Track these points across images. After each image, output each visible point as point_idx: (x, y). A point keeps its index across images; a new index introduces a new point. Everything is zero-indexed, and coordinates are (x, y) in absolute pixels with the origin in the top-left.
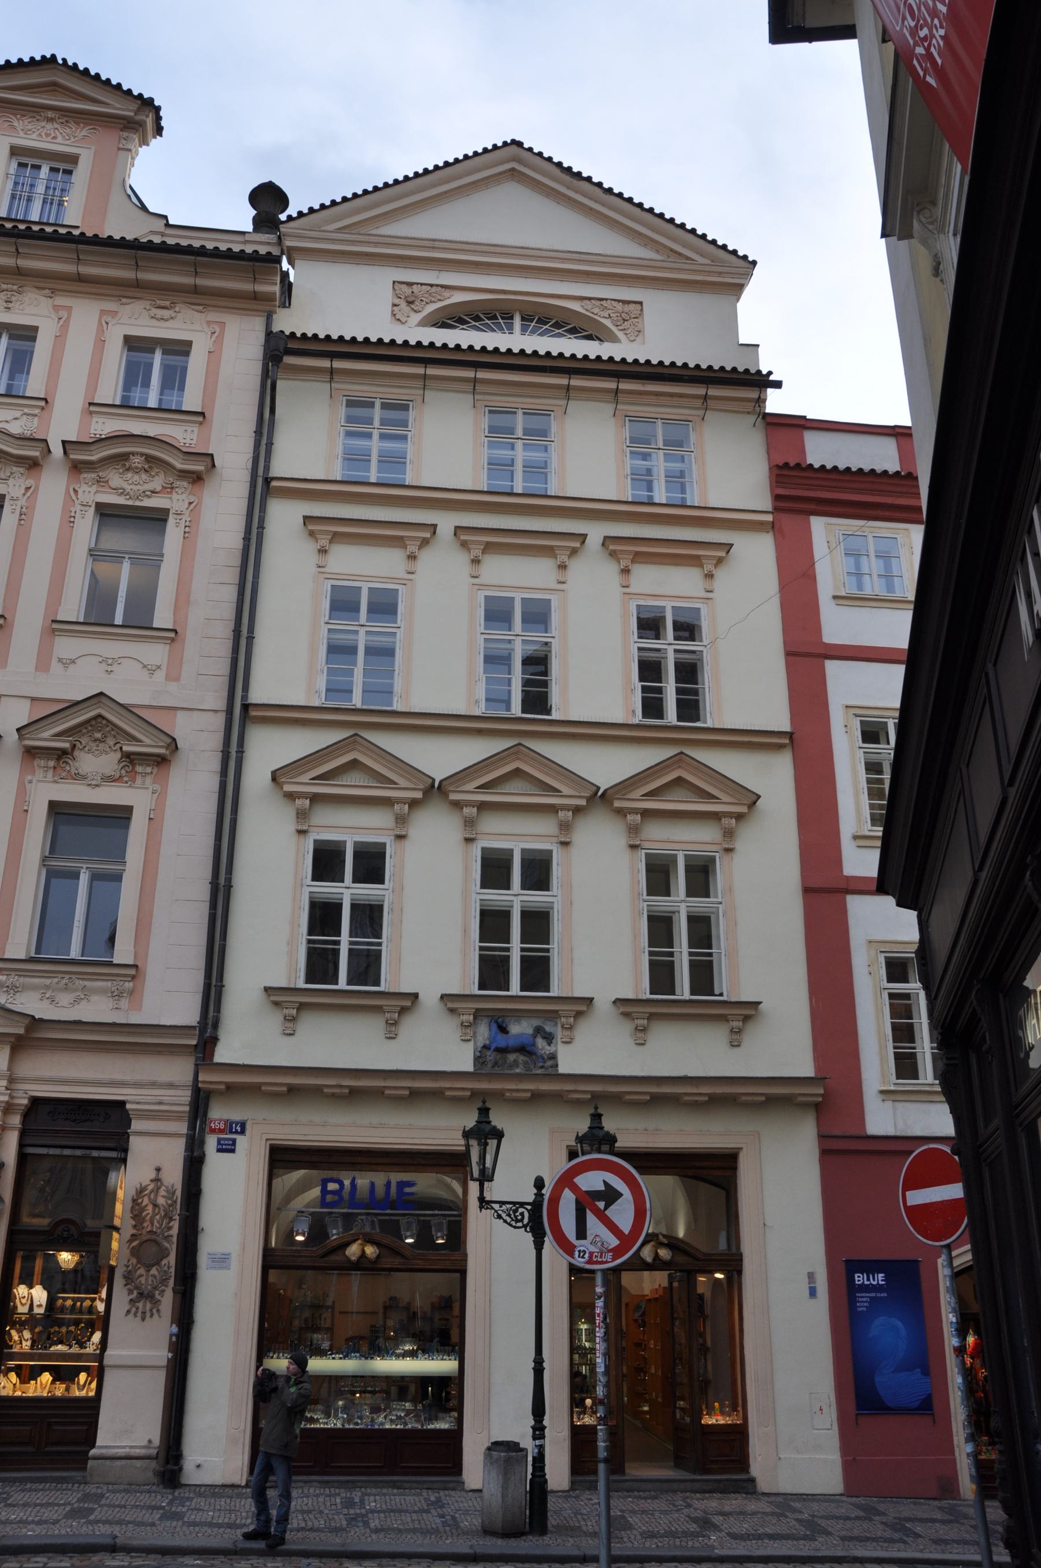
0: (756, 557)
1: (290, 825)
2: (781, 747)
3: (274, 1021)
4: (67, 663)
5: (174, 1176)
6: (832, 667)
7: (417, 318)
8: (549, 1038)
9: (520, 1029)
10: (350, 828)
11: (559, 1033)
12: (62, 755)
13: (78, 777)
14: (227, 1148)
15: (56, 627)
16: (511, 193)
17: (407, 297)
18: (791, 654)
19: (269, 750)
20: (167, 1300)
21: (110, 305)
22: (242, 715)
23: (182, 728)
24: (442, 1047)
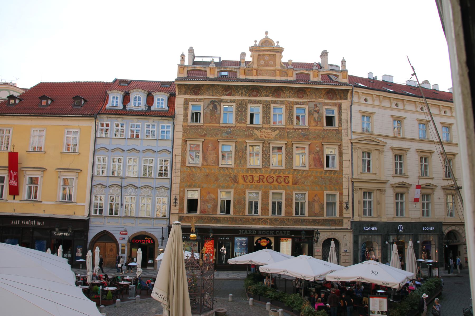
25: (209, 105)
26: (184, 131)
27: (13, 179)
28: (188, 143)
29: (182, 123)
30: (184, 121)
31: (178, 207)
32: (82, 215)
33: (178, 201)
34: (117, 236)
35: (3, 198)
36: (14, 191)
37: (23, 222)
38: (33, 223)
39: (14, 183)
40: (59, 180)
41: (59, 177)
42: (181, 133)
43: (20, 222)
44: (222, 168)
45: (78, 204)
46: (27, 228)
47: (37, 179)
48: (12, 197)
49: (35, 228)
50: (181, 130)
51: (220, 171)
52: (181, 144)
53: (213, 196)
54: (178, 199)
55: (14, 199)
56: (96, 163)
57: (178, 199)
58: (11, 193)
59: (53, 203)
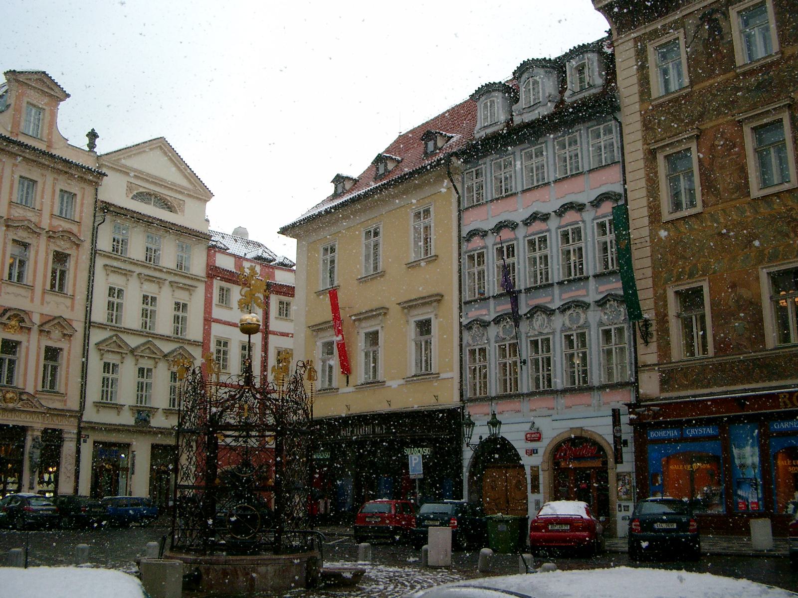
0: (201, 289)
1: (99, 357)
2: (199, 345)
3: (95, 410)
4: (48, 303)
5: (74, 449)
6: (213, 324)
7: (131, 195)
8: (149, 417)
9: (144, 415)
10: (112, 359)
11: (151, 415)
12: (48, 332)
13: (50, 339)
14: (85, 441)
15: (44, 292)
16: (158, 152)
17: (130, 188)
18: (205, 320)
19: (97, 336)
20: (73, 478)
21: (56, 176)
22: (89, 325)
23: (75, 325)
24: (127, 419)
25: (699, 27)
26: (647, 126)
28: (660, 158)
29: (637, 107)
30: (642, 101)
31: (653, 347)
32: (450, 398)
33: (653, 329)
34: (521, 446)
42: (639, 135)
44: (764, 198)
45: (442, 376)
47: (377, 332)
50: (638, 126)
51: (756, 212)
52: (641, 164)
53: (745, 293)
54: (654, 323)
56: (465, 271)
57: (654, 323)
59: (402, 382)
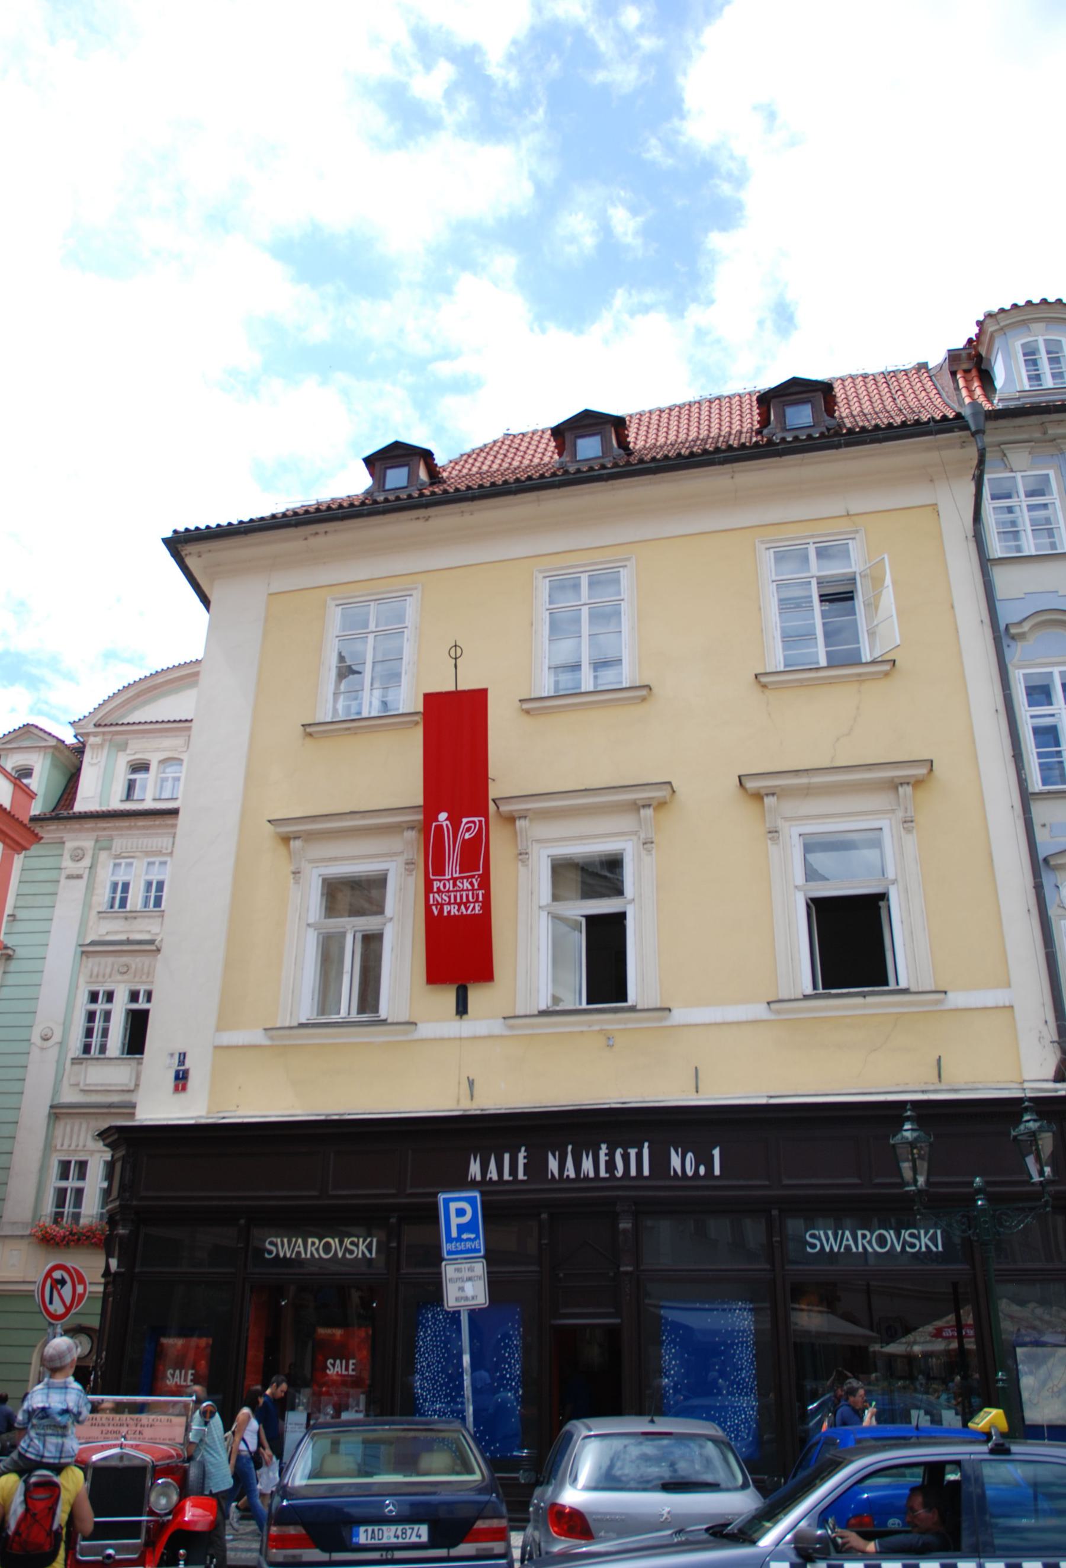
27: (452, 869)
35: (383, 1013)
36: (460, 955)
37: (553, 1165)
38: (635, 1161)
39: (456, 896)
40: (772, 849)
41: (774, 832)
43: (537, 1166)
45: (957, 999)
46: (597, 1204)
48: (448, 997)
49: (661, 1200)
55: (462, 1009)
56: (1027, 716)
58: (438, 970)
59: (759, 1011)
